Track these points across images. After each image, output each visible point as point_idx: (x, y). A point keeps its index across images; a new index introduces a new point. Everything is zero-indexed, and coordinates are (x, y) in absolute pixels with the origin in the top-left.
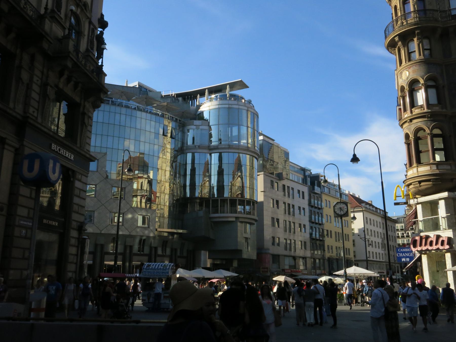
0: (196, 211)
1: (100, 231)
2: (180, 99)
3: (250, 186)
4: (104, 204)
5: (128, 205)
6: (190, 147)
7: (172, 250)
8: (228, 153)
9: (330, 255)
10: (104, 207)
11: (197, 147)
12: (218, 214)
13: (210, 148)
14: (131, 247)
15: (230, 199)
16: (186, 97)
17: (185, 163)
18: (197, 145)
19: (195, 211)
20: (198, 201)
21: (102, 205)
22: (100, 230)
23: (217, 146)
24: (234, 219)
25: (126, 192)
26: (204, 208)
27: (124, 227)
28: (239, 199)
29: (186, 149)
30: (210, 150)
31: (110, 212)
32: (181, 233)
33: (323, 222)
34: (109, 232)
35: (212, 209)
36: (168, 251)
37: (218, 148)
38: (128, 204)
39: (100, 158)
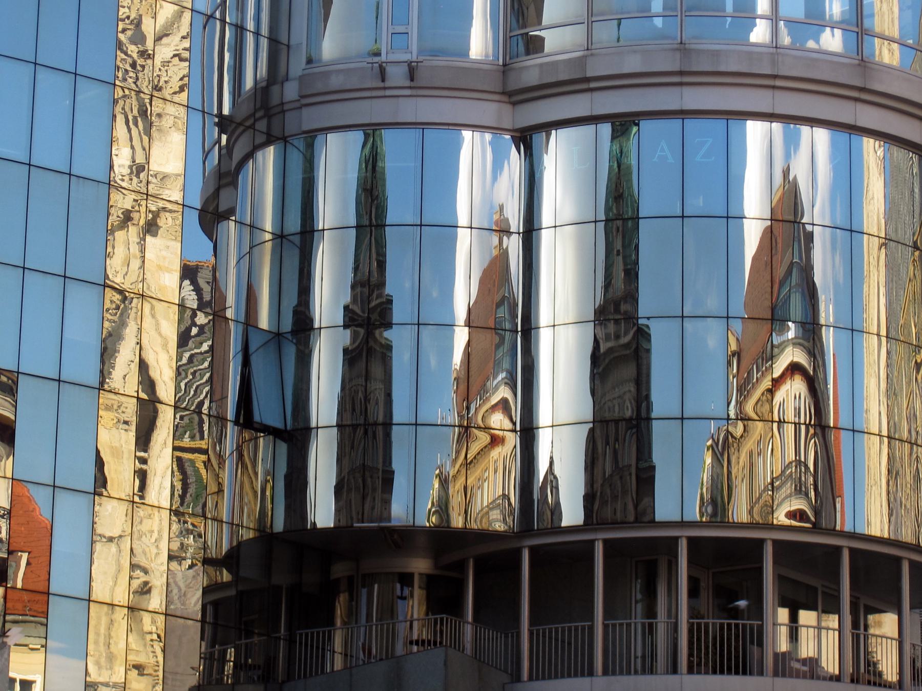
0: (400, 649)
3: (893, 426)
6: (336, 82)
8: (676, 124)
11: (396, 75)
12: (587, 680)
13: (512, 86)
15: (691, 541)
17: (294, 224)
18: (392, 58)
19: (389, 655)
20: (420, 565)
23: (581, 62)
26: (468, 630)
28: (775, 542)
30: (514, 104)
35: (531, 633)
37: (588, 80)
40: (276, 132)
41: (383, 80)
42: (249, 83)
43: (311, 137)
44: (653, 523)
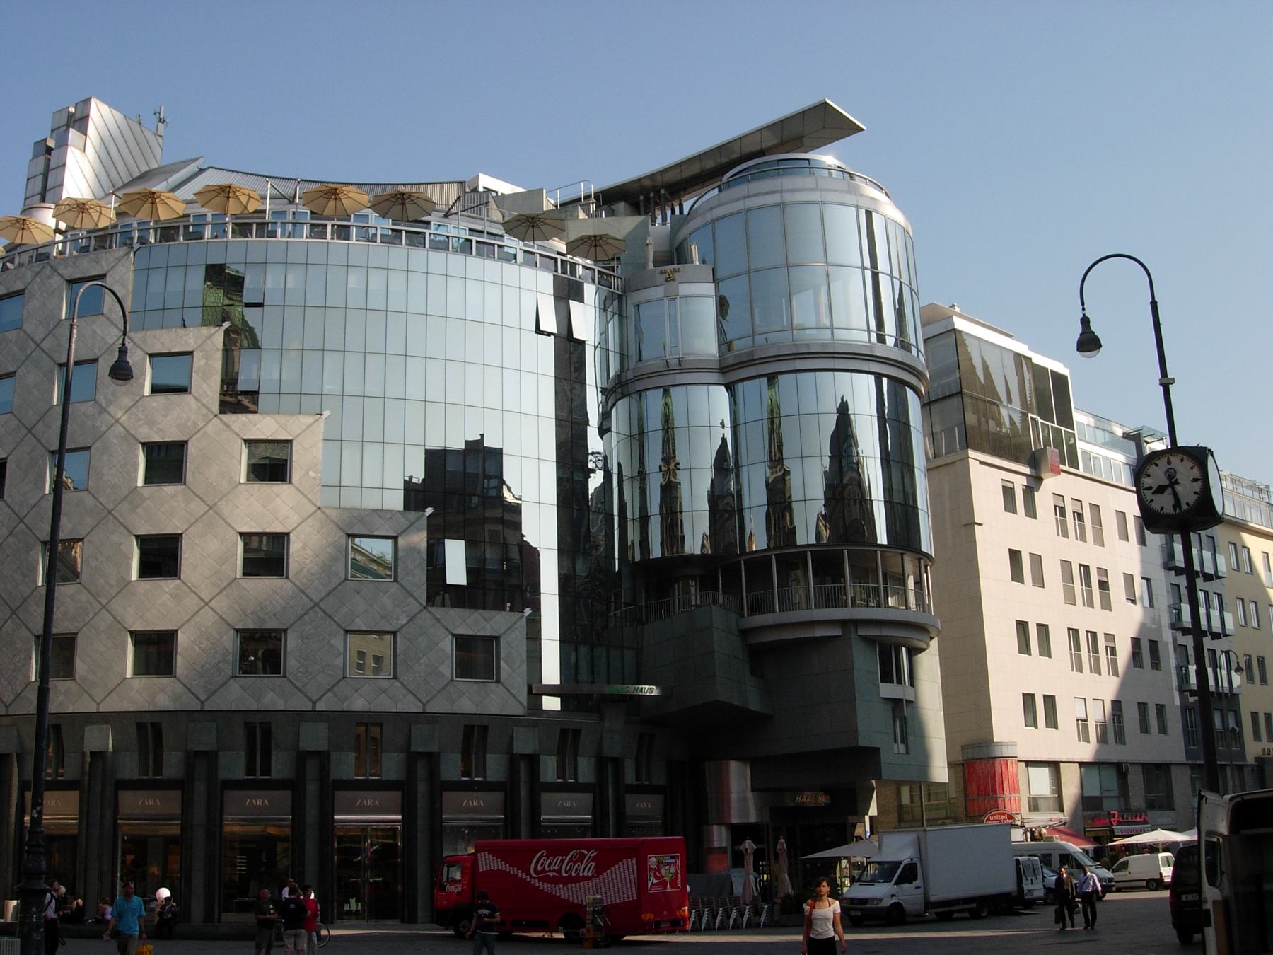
1: (310, 704)
2: (621, 206)
4: (321, 600)
5: (411, 599)
7: (601, 762)
9: (1264, 750)
10: (321, 614)
11: (674, 364)
12: (771, 614)
14: (432, 759)
16: (642, 198)
17: (635, 431)
18: (671, 357)
21: (312, 608)
22: (310, 699)
23: (751, 353)
24: (836, 632)
25: (400, 554)
26: (721, 597)
27: (402, 683)
29: (638, 378)
30: (724, 373)
31: (347, 632)
32: (632, 697)
33: (1227, 627)
34: (345, 707)
36: (585, 770)
38: (412, 595)
39: (297, 436)
40: (625, 393)
41: (668, 366)
42: (612, 374)
43: (640, 393)
44: (795, 546)
